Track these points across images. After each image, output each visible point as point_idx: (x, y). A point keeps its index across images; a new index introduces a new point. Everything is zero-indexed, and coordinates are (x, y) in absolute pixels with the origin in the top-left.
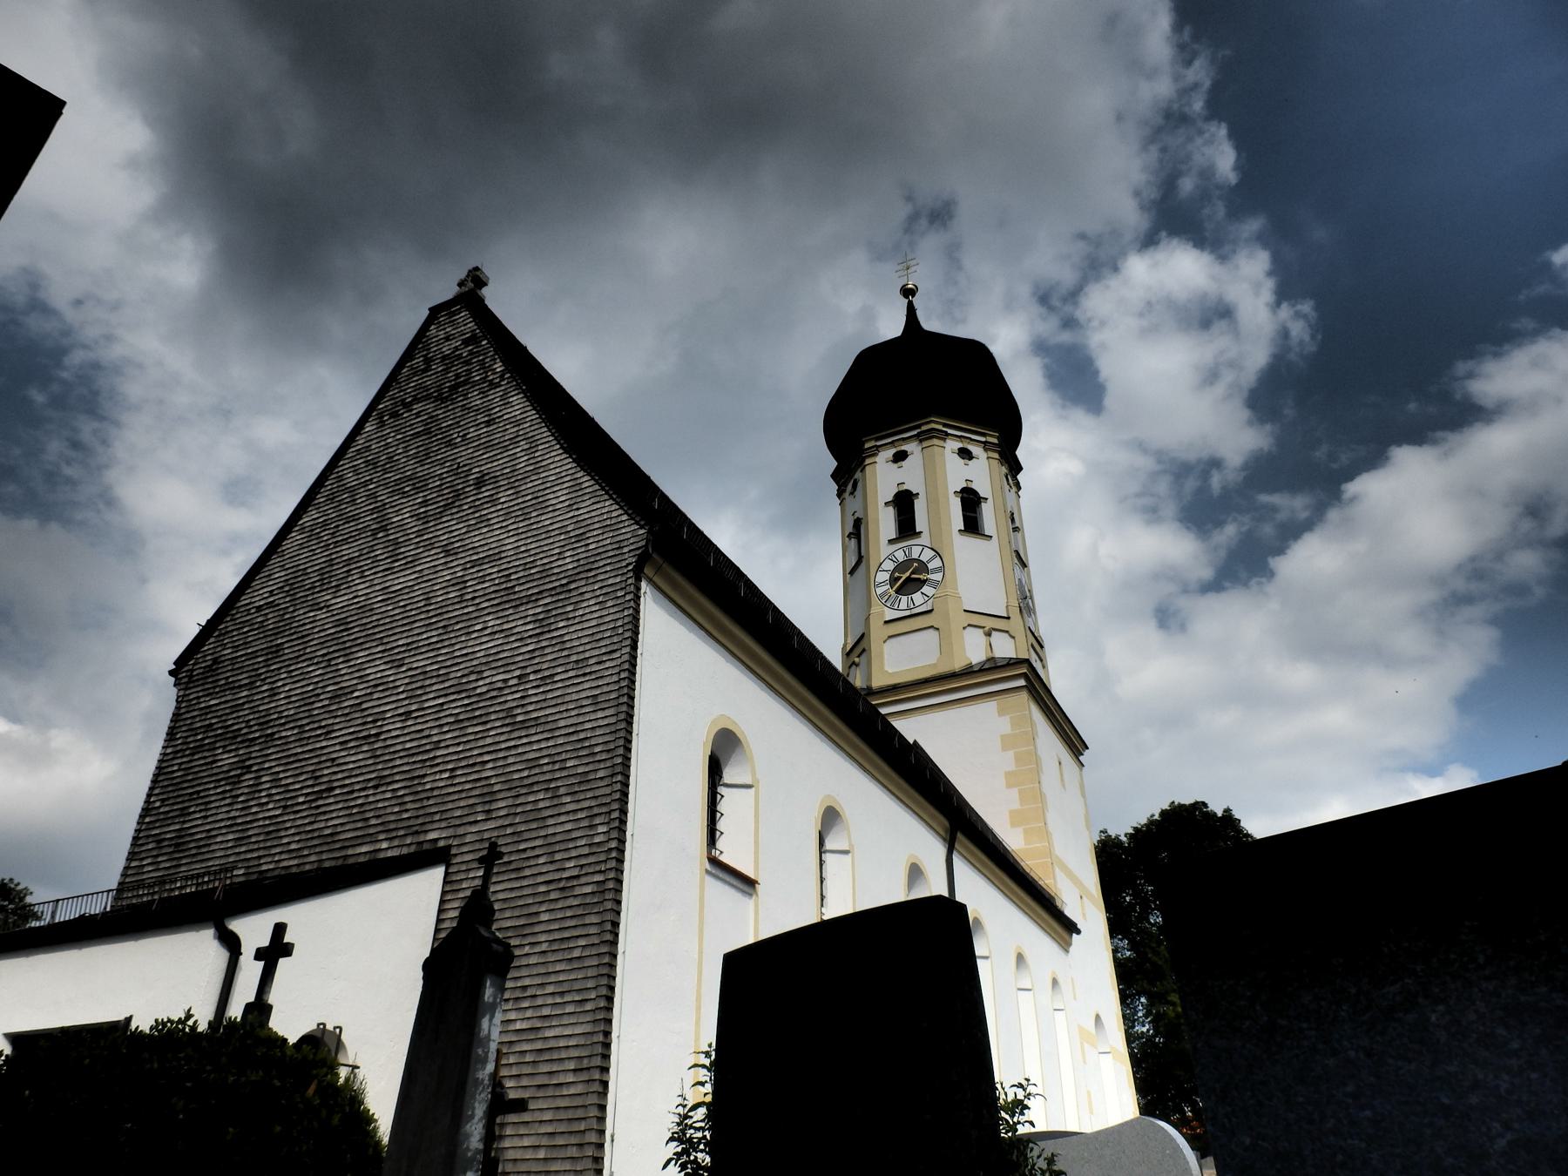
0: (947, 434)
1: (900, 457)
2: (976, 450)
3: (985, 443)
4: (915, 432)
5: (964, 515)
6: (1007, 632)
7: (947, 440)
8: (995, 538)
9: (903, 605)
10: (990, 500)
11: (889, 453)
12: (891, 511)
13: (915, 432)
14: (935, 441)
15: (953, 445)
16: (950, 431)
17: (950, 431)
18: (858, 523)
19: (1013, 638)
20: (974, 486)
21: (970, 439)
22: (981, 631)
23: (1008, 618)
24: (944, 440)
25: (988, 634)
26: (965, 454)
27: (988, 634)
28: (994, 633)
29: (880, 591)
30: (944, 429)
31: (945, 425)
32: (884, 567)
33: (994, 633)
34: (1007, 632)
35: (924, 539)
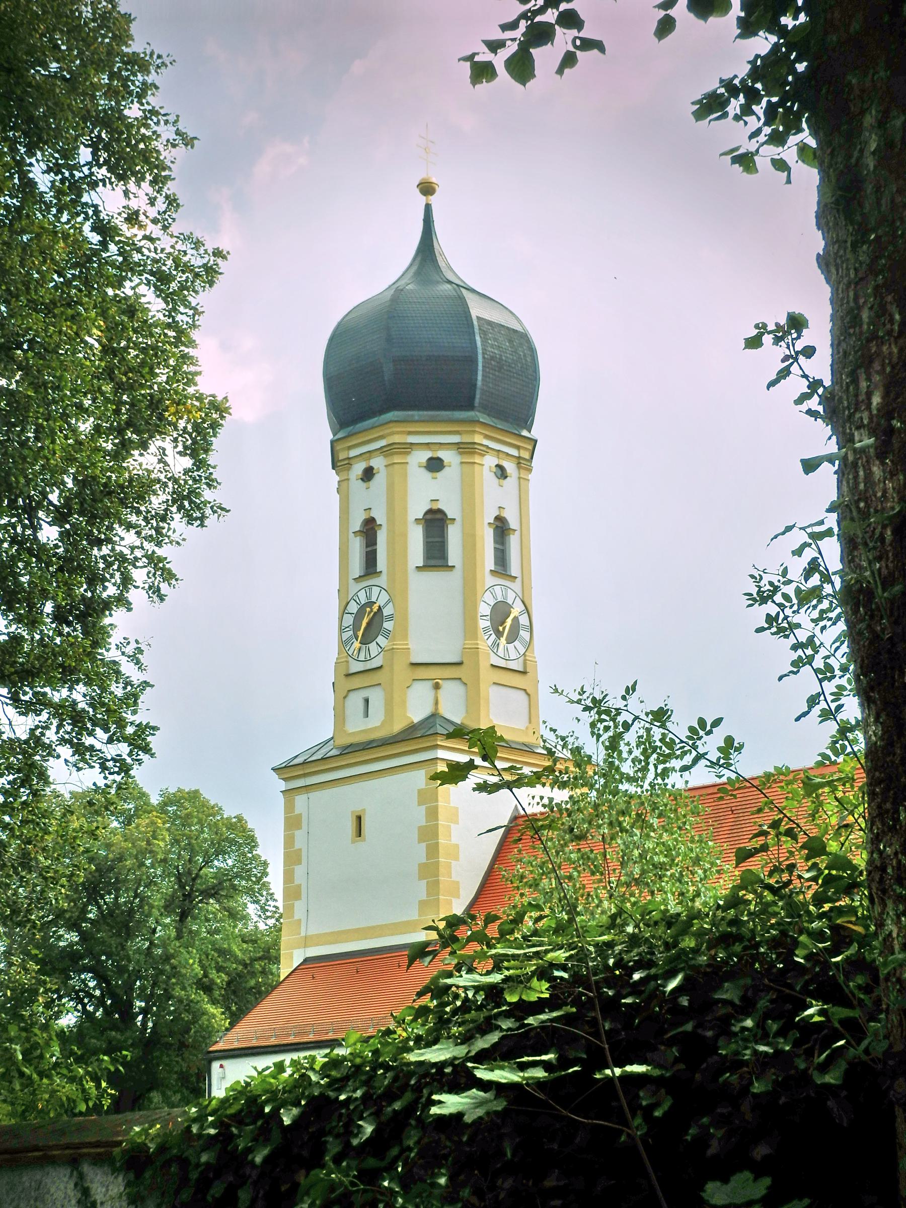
1: (435, 465)
3: (519, 458)
4: (455, 439)
6: (525, 690)
8: (518, 581)
10: (517, 533)
11: (423, 456)
13: (455, 439)
15: (490, 461)
18: (369, 529)
19: (528, 695)
20: (504, 514)
21: (507, 454)
23: (524, 673)
26: (501, 472)
30: (486, 442)
31: (487, 437)
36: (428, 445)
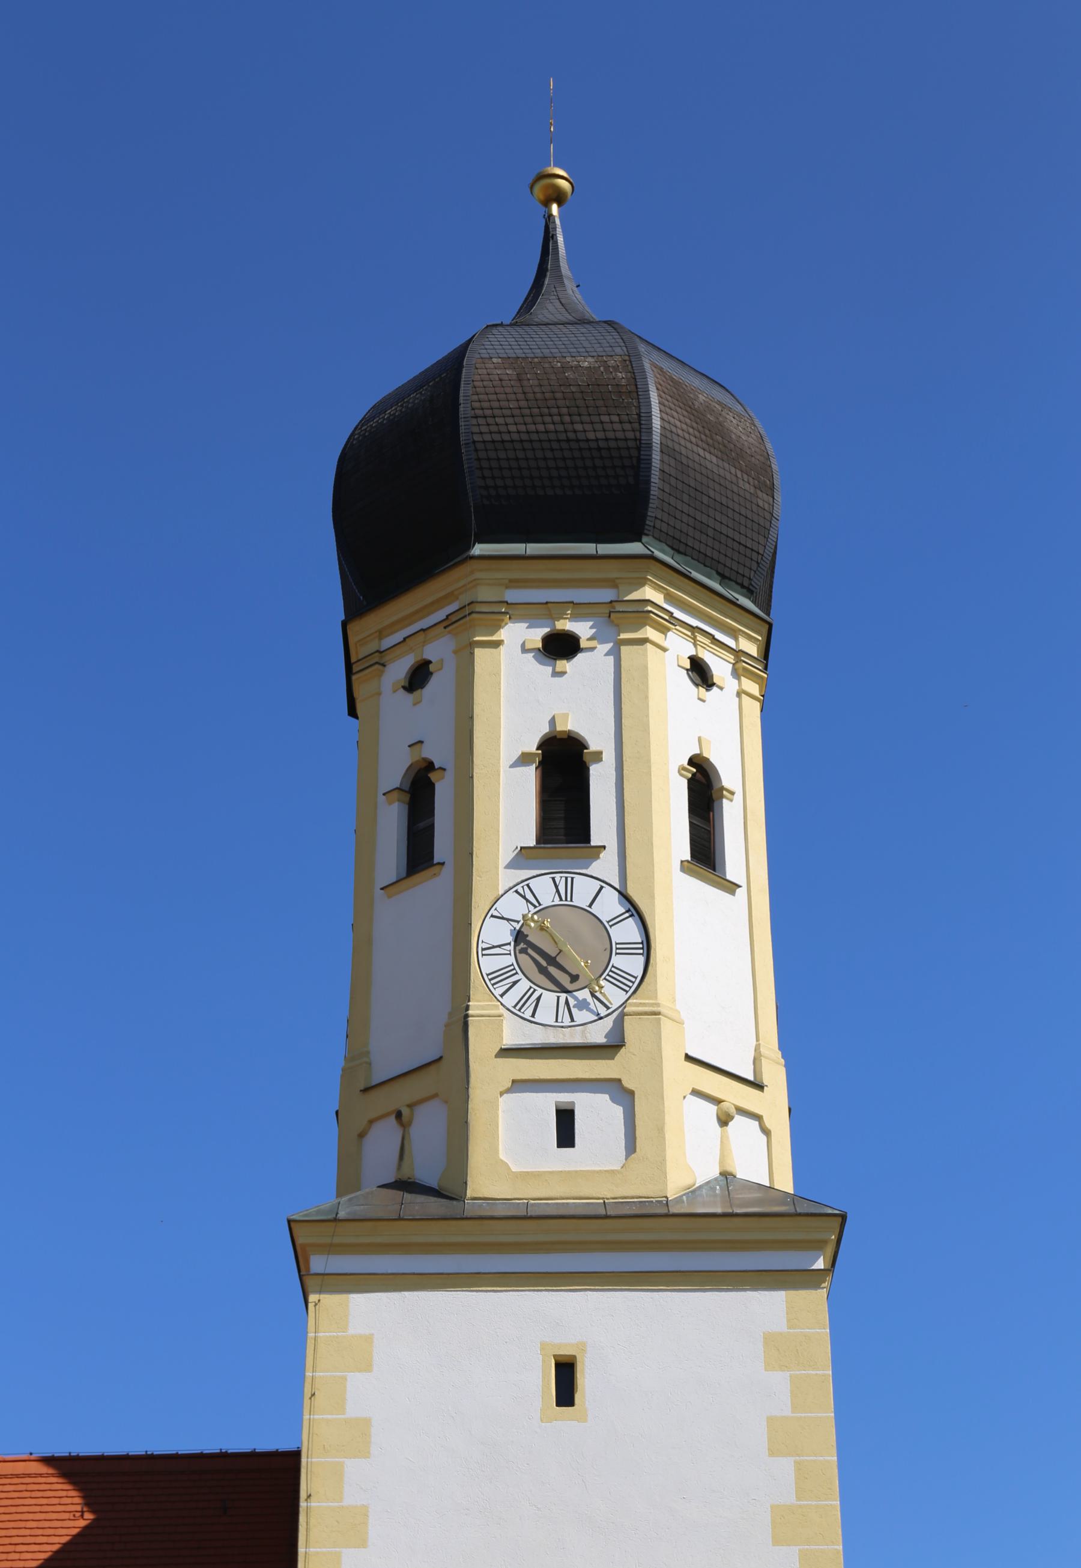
0: (674, 620)
2: (720, 667)
5: (691, 823)
6: (758, 1118)
7: (670, 634)
8: (741, 893)
9: (545, 1014)
12: (529, 778)
14: (650, 633)
16: (678, 614)
17: (678, 614)
19: (766, 1132)
22: (713, 1109)
23: (759, 1086)
24: (664, 631)
25: (724, 1121)
26: (700, 672)
27: (724, 1121)
28: (739, 1120)
29: (489, 964)
32: (502, 907)
33: (739, 1120)
34: (758, 1118)
35: (606, 866)
36: (548, 610)
